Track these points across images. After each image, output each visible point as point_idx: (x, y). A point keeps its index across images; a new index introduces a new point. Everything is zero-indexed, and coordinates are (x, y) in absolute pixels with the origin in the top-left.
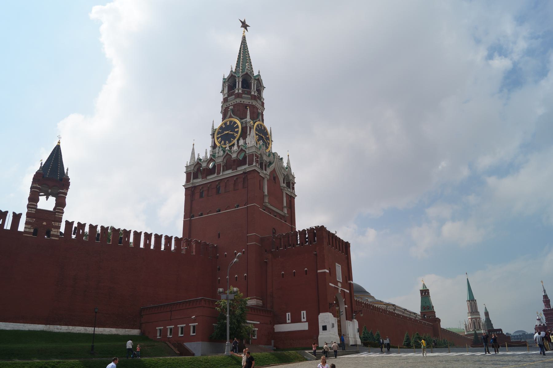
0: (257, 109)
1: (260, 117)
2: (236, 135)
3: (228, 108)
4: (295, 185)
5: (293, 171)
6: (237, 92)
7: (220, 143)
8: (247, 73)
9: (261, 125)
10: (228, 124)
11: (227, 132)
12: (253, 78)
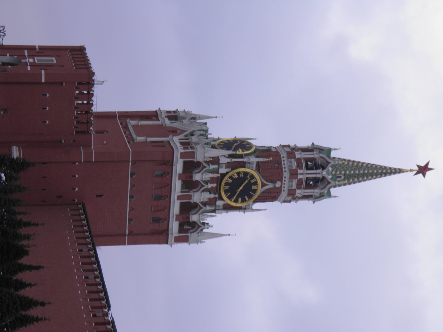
0: (281, 180)
1: (270, 186)
5: (209, 242)
6: (296, 153)
7: (221, 142)
8: (328, 163)
9: (256, 183)
10: (247, 146)
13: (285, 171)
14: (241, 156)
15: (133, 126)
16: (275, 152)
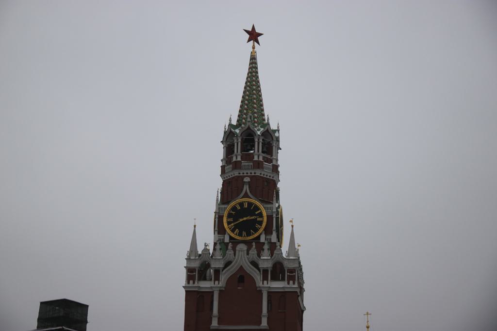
2: (257, 226)
3: (240, 179)
4: (304, 293)
6: (256, 158)
7: (233, 231)
8: (267, 130)
10: (246, 206)
11: (245, 219)
12: (275, 139)
13: (273, 177)
14: (270, 218)
15: (219, 323)
16: (251, 179)
